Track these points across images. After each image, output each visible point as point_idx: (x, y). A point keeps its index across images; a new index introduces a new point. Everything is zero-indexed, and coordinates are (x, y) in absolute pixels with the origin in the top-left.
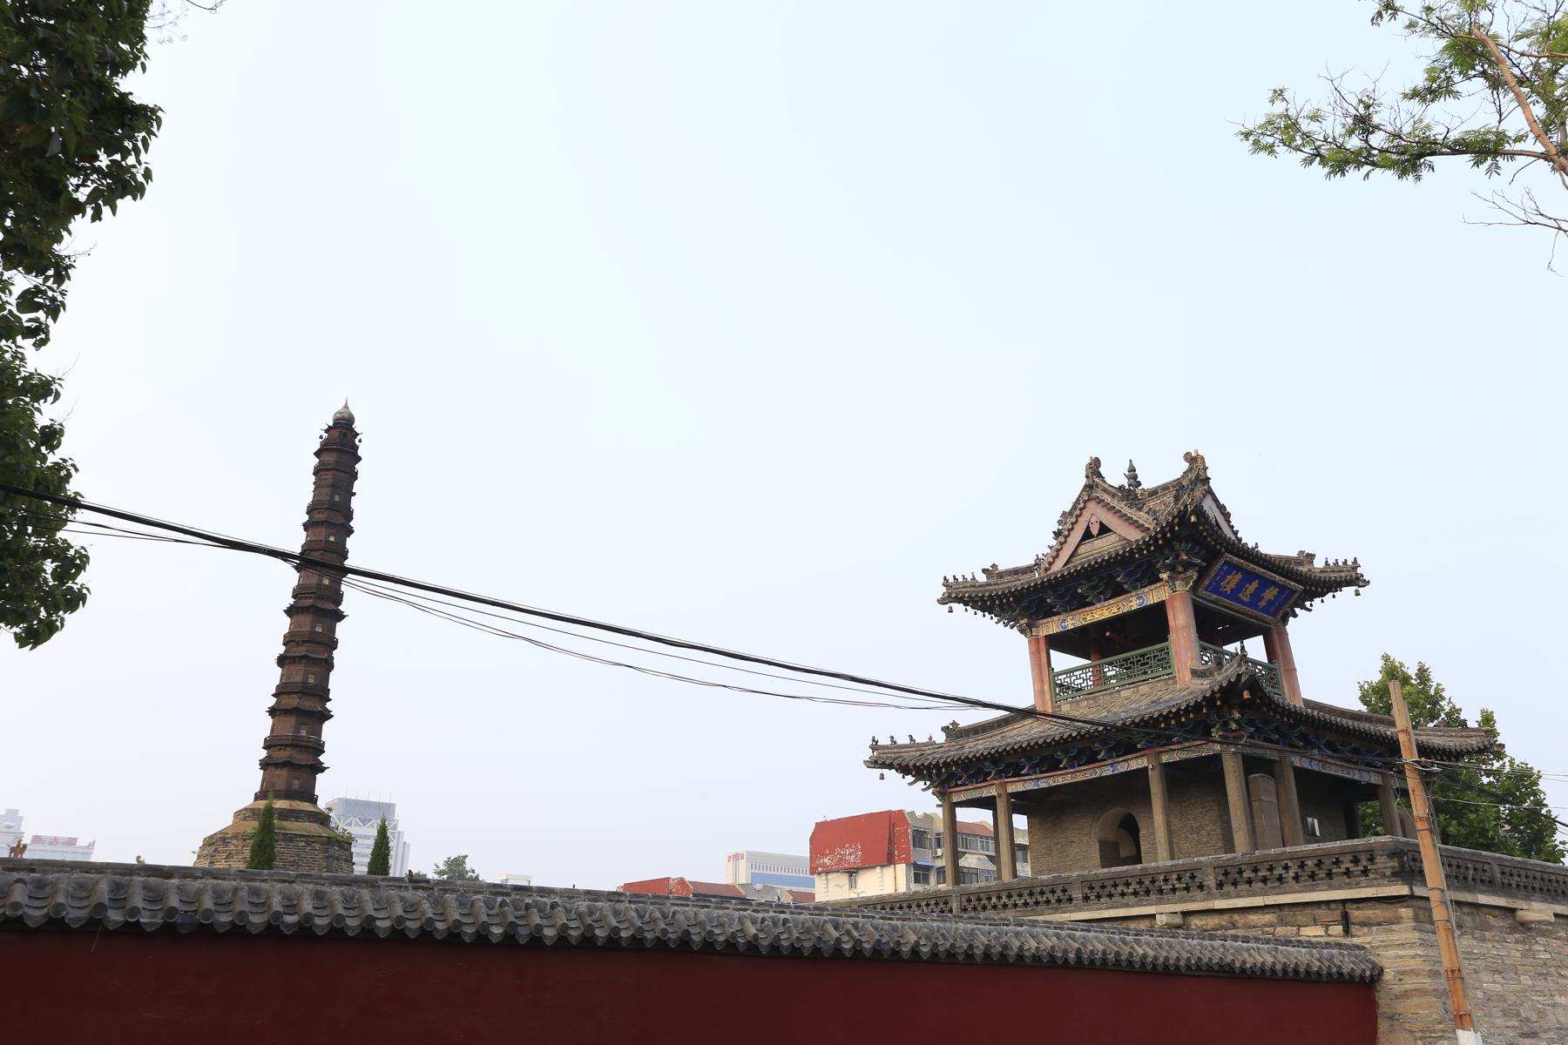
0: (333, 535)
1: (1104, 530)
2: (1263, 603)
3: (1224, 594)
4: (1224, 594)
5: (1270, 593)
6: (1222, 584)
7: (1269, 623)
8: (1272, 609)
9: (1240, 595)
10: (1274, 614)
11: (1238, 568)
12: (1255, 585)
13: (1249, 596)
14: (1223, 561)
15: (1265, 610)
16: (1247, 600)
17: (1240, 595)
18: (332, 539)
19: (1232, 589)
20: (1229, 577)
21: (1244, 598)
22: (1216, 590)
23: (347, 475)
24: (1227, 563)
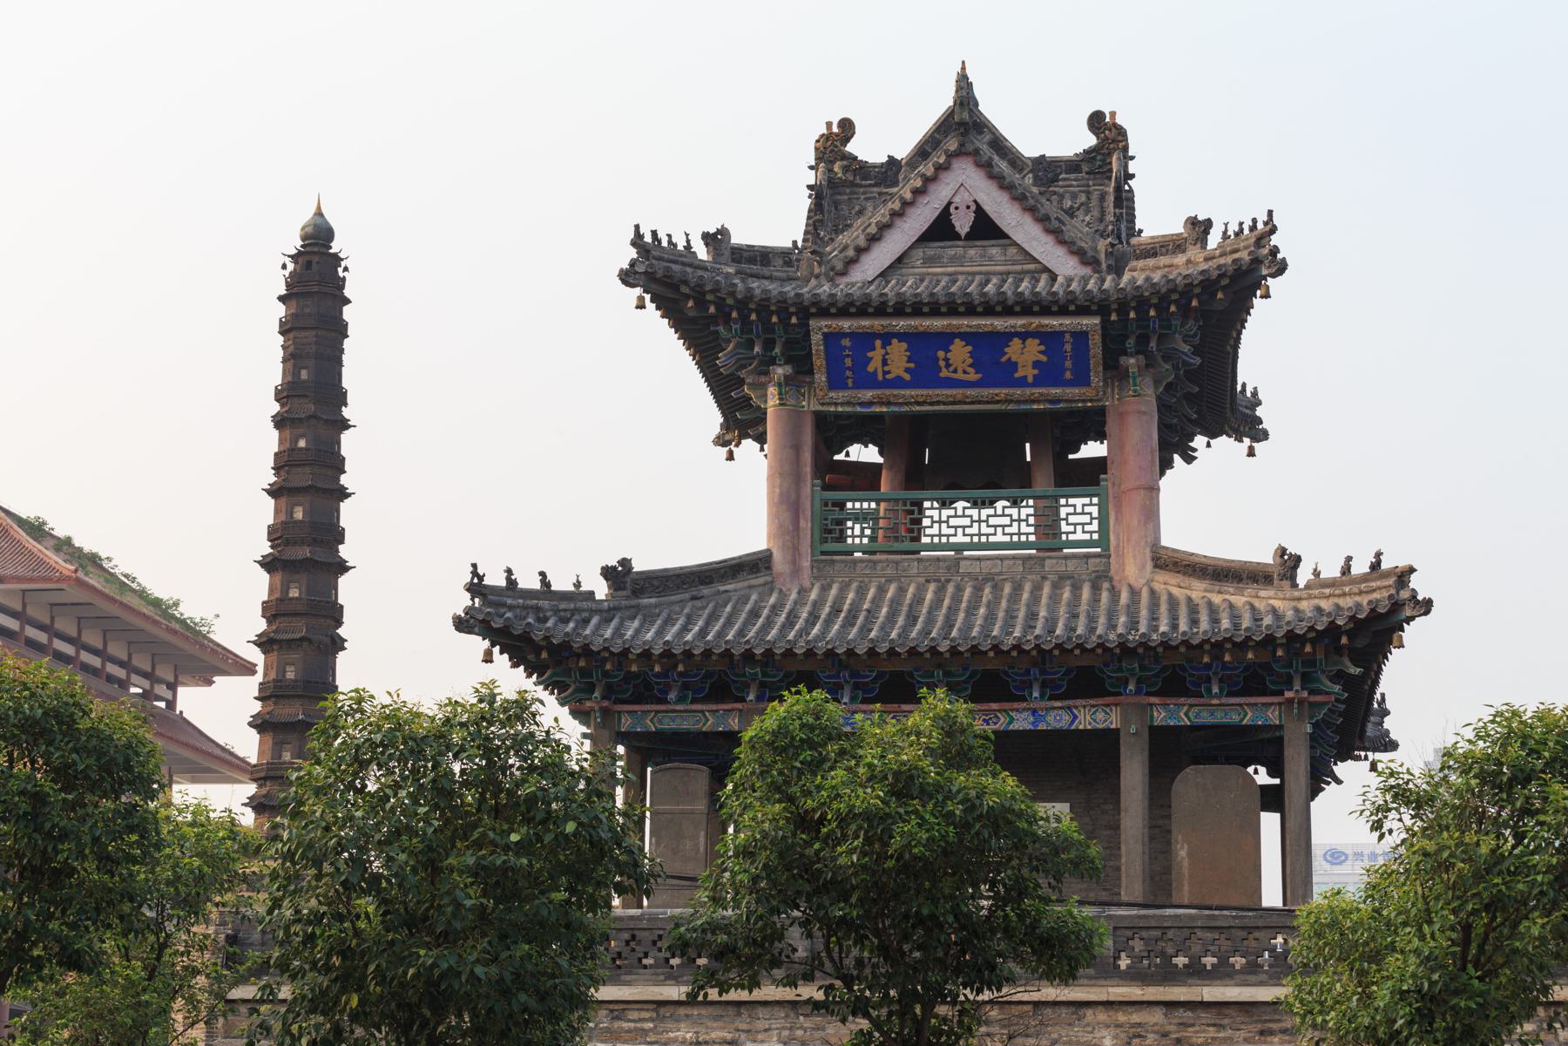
0: (302, 436)
1: (985, 229)
2: (1030, 373)
3: (898, 383)
4: (898, 383)
5: (1025, 355)
6: (871, 369)
7: (1098, 400)
8: (1068, 375)
9: (944, 373)
10: (1082, 379)
11: (887, 338)
12: (960, 353)
13: (971, 370)
14: (816, 338)
15: (1038, 382)
16: (973, 376)
17: (944, 373)
18: (302, 444)
19: (907, 370)
20: (876, 355)
21: (960, 376)
22: (870, 382)
23: (313, 333)
24: (831, 338)
